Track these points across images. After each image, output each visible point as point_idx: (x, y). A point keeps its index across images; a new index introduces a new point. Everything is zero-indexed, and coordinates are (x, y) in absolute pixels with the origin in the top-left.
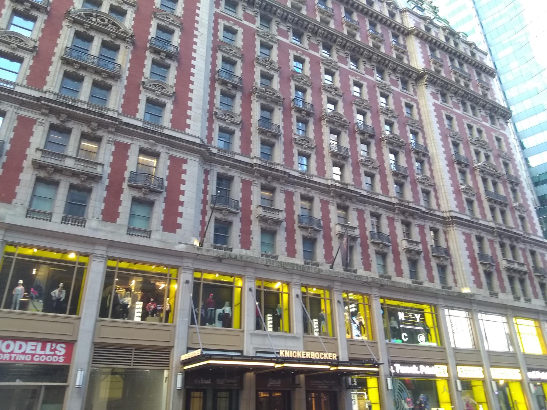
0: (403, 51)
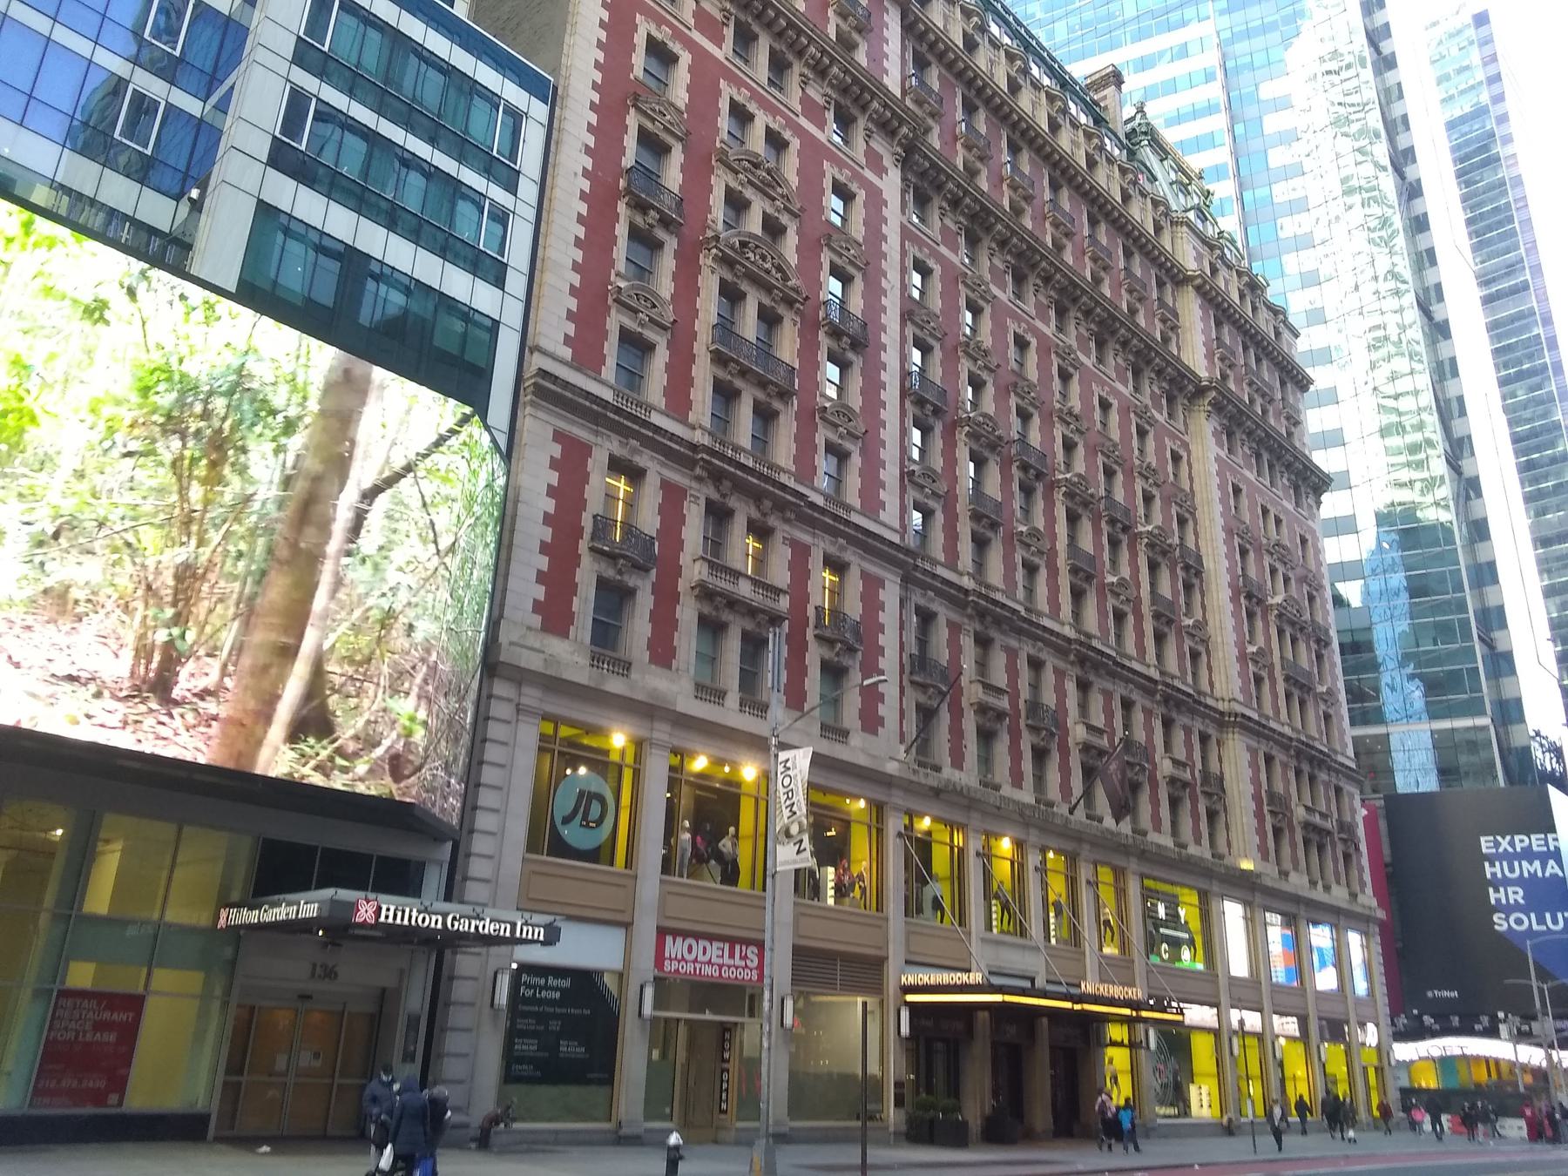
0: (1171, 323)
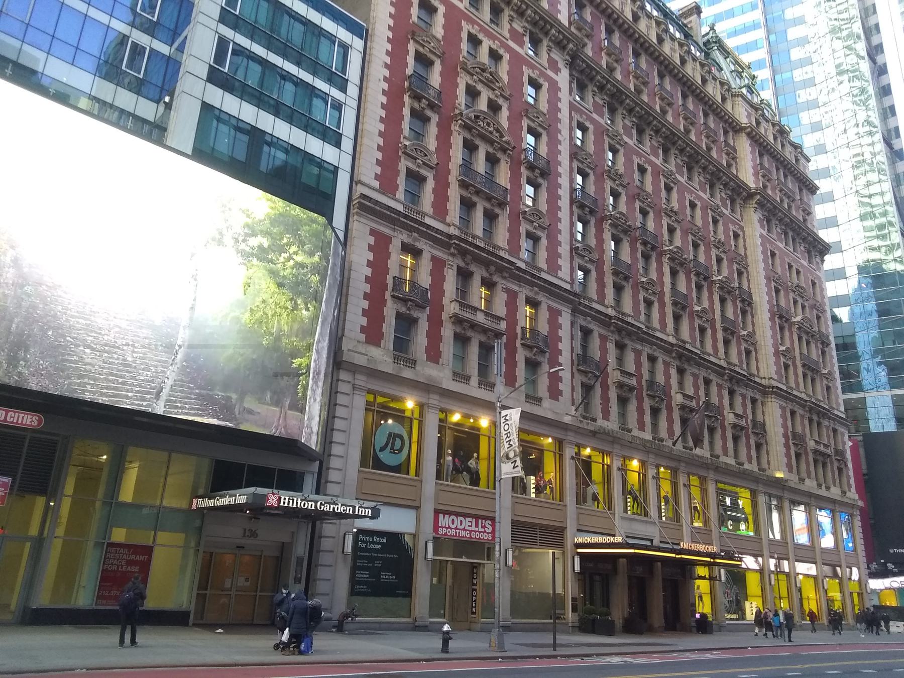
0: (733, 155)
